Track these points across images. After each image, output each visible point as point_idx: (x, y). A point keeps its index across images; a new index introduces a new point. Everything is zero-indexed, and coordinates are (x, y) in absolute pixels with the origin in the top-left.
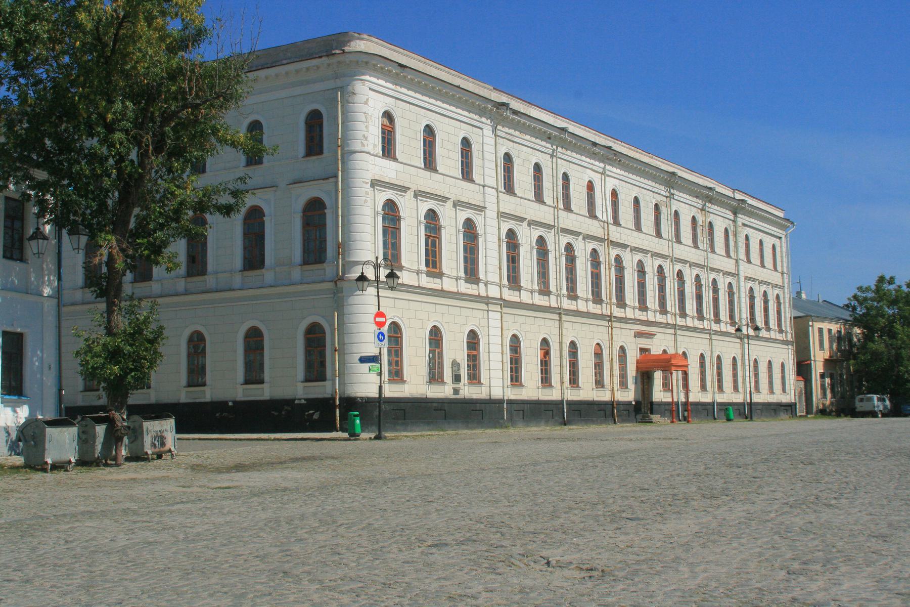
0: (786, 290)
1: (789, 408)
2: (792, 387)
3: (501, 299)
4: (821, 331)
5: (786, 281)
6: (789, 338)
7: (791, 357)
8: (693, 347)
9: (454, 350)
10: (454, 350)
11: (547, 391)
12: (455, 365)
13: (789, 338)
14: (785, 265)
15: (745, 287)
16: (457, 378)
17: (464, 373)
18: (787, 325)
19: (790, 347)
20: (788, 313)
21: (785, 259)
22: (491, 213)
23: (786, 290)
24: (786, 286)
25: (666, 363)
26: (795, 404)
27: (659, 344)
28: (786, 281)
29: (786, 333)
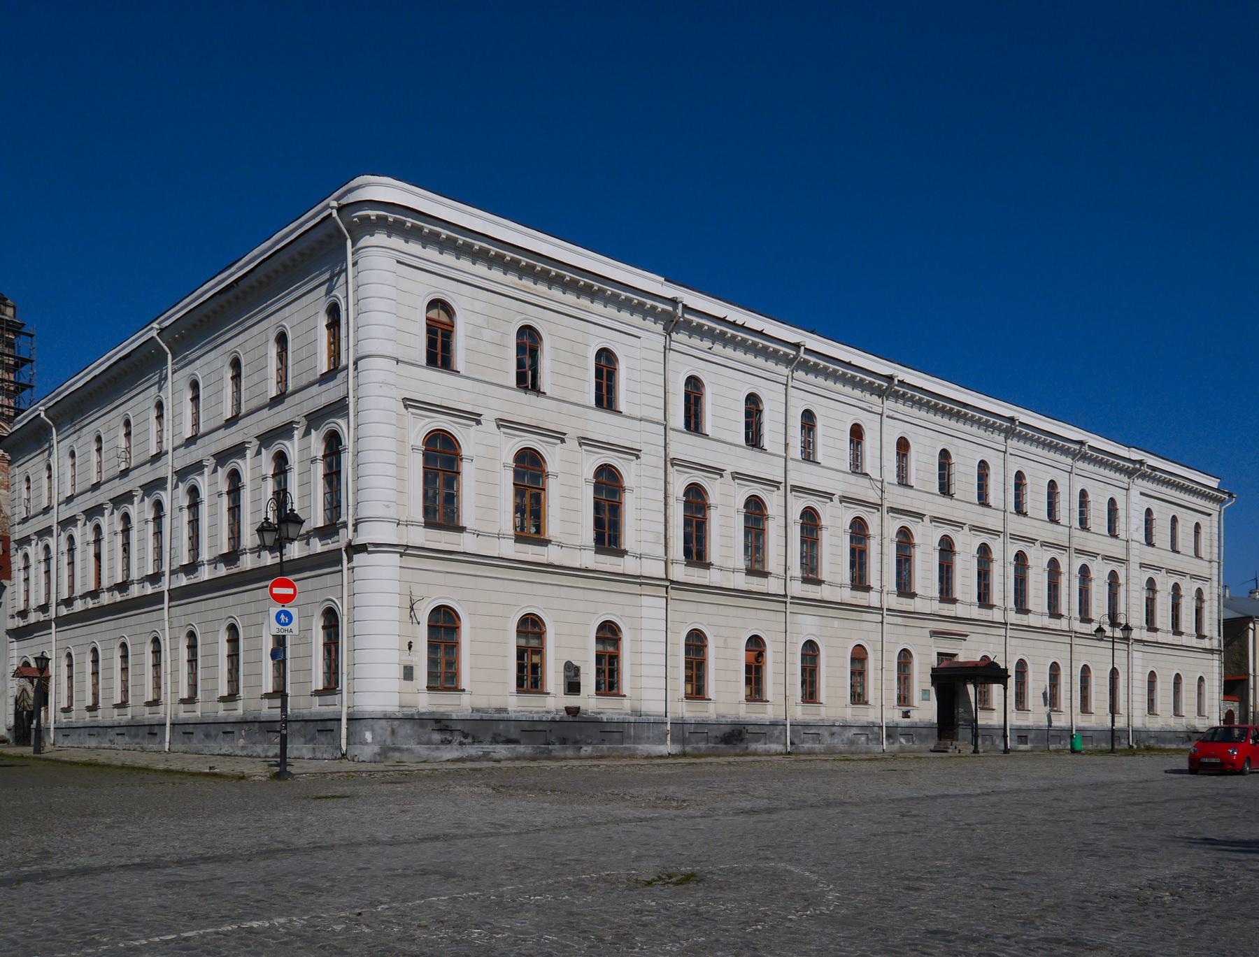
3: (667, 579)
6: (1215, 645)
7: (1216, 670)
8: (1038, 656)
10: (568, 644)
11: (756, 706)
13: (1215, 645)
15: (1164, 585)
18: (1211, 627)
19: (1216, 656)
22: (653, 457)
25: (989, 673)
27: (968, 652)
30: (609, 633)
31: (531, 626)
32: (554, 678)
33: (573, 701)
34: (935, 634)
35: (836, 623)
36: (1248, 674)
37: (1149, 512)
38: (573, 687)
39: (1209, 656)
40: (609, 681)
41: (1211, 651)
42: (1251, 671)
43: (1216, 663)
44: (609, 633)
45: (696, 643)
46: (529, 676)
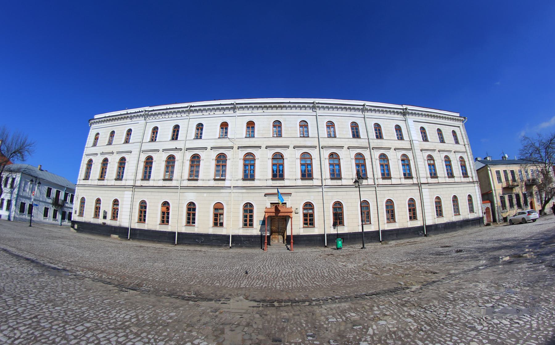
0: (469, 154)
1: (478, 221)
2: (480, 208)
4: (498, 172)
5: (468, 149)
7: (477, 190)
9: (107, 207)
10: (107, 207)
12: (105, 213)
13: (475, 180)
14: (465, 140)
16: (105, 217)
17: (109, 216)
20: (472, 167)
21: (464, 137)
23: (469, 154)
24: (468, 151)
26: (483, 217)
28: (468, 149)
29: (472, 178)
30: (116, 202)
31: (98, 201)
32: (101, 214)
33: (104, 221)
34: (266, 195)
35: (205, 195)
36: (492, 190)
37: (422, 129)
38: (105, 217)
39: (473, 185)
40: (115, 215)
41: (473, 182)
42: (493, 189)
43: (477, 188)
44: (116, 202)
45: (143, 206)
46: (97, 215)
